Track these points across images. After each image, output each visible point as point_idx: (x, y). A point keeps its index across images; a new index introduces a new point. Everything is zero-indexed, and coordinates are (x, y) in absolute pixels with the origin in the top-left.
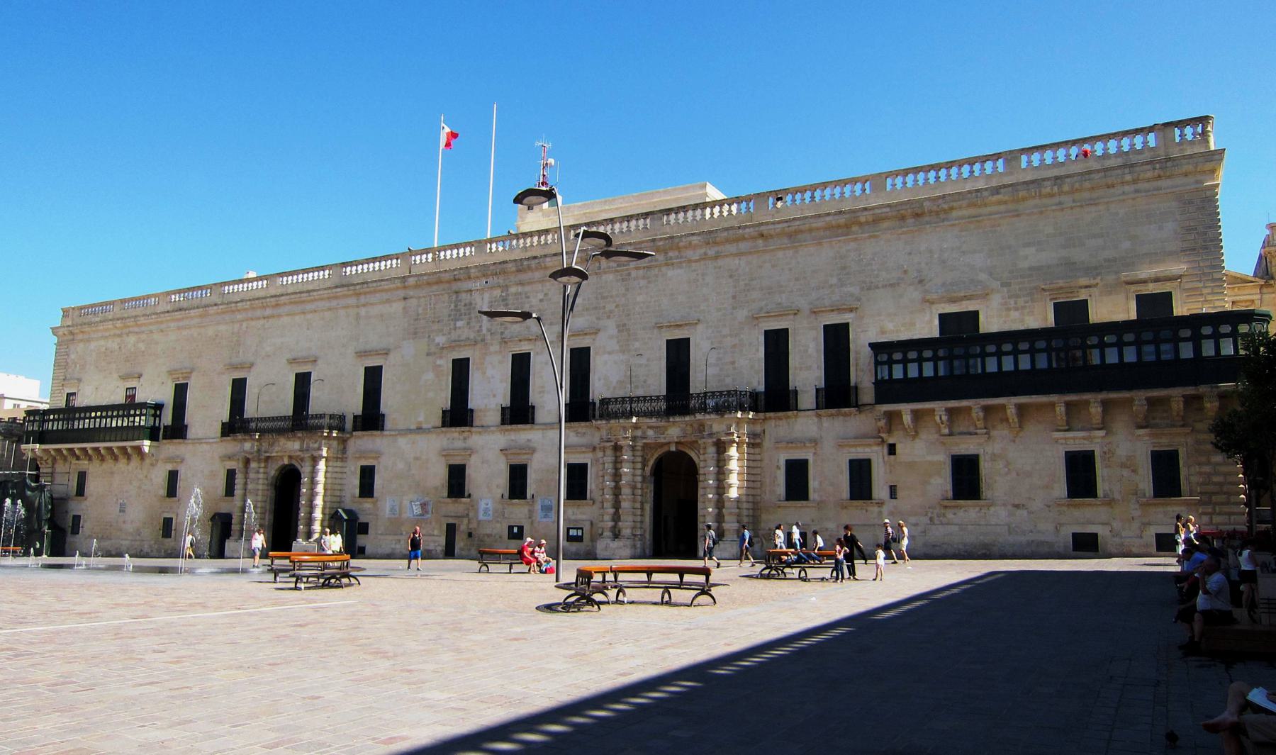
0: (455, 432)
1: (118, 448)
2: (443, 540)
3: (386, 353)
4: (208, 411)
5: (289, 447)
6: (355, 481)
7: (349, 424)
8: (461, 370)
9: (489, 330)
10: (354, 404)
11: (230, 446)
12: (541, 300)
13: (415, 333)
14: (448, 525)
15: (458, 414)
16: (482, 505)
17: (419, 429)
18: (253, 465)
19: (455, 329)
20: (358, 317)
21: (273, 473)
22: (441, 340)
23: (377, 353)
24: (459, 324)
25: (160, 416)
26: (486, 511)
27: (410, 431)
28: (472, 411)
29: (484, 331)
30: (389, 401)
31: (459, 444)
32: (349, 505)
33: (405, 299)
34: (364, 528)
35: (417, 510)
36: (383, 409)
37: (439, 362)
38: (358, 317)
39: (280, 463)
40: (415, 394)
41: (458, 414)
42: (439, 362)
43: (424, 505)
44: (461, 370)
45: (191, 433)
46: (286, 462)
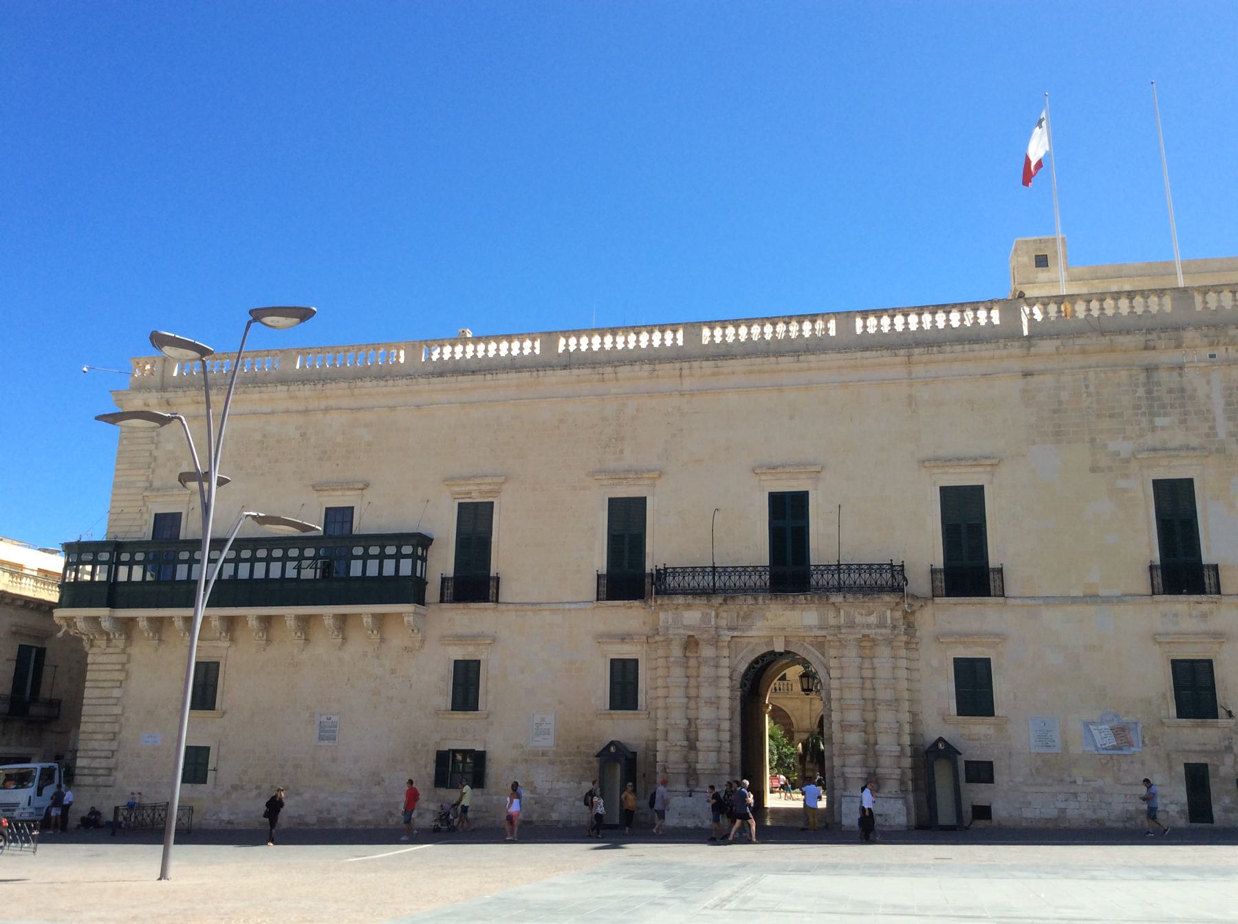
0: (1182, 606)
1: (86, 619)
3: (993, 462)
5: (783, 622)
6: (941, 690)
7: (919, 582)
11: (628, 616)
17: (1121, 599)
18: (707, 652)
19: (1153, 429)
20: (911, 401)
21: (743, 667)
23: (976, 461)
24: (1159, 421)
25: (424, 559)
27: (1074, 600)
28: (1215, 568)
29: (1222, 433)
31: (1189, 624)
32: (934, 729)
33: (1027, 374)
35: (1104, 737)
36: (993, 561)
37: (1122, 483)
38: (911, 401)
42: (1122, 483)
43: (1120, 731)
45: (507, 592)
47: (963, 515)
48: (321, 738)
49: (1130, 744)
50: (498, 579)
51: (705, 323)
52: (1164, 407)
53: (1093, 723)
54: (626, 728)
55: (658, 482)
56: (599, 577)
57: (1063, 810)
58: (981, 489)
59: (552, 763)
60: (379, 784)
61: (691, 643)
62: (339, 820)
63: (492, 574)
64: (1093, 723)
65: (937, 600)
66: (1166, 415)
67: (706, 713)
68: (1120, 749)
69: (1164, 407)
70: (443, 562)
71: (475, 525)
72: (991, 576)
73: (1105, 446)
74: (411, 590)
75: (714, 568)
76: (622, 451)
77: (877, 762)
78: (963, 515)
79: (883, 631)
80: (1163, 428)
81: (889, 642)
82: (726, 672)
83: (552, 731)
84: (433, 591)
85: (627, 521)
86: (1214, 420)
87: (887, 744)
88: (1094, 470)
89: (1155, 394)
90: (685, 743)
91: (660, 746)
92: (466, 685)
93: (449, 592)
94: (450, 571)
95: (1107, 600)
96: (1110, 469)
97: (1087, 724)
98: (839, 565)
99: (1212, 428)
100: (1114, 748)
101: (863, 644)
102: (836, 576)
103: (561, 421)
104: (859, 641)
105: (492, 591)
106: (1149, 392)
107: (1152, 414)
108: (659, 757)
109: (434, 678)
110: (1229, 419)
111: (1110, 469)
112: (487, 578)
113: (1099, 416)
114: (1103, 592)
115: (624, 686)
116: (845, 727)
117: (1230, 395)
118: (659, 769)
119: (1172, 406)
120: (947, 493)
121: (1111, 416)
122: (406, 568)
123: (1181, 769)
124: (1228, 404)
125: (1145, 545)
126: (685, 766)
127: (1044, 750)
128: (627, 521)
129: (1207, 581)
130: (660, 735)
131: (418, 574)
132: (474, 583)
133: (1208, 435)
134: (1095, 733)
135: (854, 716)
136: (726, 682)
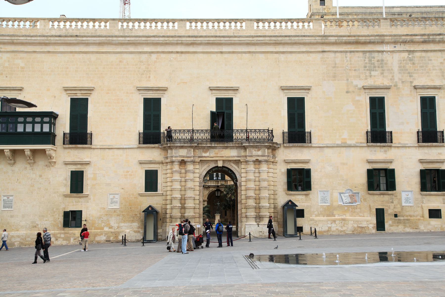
2: (374, 220)
4: (116, 123)
7: (278, 139)
8: (377, 107)
9: (400, 79)
10: (280, 125)
12: (441, 63)
13: (334, 77)
14: (377, 210)
15: (378, 134)
16: (404, 195)
18: (190, 167)
19: (371, 76)
22: (361, 83)
24: (373, 73)
25: (54, 125)
26: (407, 200)
29: (396, 79)
30: (311, 123)
34: (301, 213)
35: (346, 198)
36: (307, 129)
37: (357, 98)
39: (213, 165)
40: (338, 121)
41: (378, 134)
42: (357, 98)
43: (351, 197)
44: (377, 107)
45: (96, 141)
46: (220, 164)
47: (296, 108)
48: (4, 207)
49: (356, 201)
50: (91, 134)
51: (188, 20)
52: (375, 67)
53: (342, 193)
54: (154, 201)
55: (166, 92)
56: (139, 133)
57: (330, 227)
58: (304, 98)
59: (118, 215)
60: (35, 227)
61: (183, 163)
62: (16, 243)
63: (89, 131)
64: (342, 193)
65: (285, 145)
66: (376, 71)
67: (189, 194)
68: (352, 203)
69: (375, 67)
70: (63, 126)
71: (79, 108)
72: (306, 135)
73: (352, 82)
74: (49, 138)
75: (193, 130)
76: (149, 77)
77: (260, 211)
78: (296, 108)
79: (264, 158)
80: (375, 76)
81: (266, 161)
82: (197, 175)
83: (119, 202)
84: (59, 139)
85: (152, 108)
86: (394, 73)
87: (265, 203)
88: (347, 92)
89: (373, 62)
90: (180, 205)
91: (169, 207)
92: (77, 182)
93: (67, 139)
94: (68, 131)
95: (350, 146)
96: (353, 92)
97: (340, 194)
98: (247, 130)
99: (393, 76)
100: (350, 203)
101: (256, 163)
102: (245, 134)
103: (120, 61)
104: (254, 162)
105: (89, 139)
106: (370, 61)
107: (370, 70)
108: (168, 211)
109: (61, 178)
110: (400, 73)
111: (353, 92)
112: (86, 134)
113: (350, 70)
114: (349, 142)
115: (151, 181)
116: (247, 198)
117: (401, 63)
118: (168, 216)
119: (379, 67)
120: (290, 100)
121: (355, 70)
122: (46, 128)
123: (374, 211)
124: (400, 67)
125: (365, 124)
126: (180, 215)
127: (324, 204)
128: (152, 108)
129: (387, 137)
130: (168, 202)
131: (52, 131)
132: (79, 135)
133: (391, 79)
134: (343, 197)
135: (251, 193)
136: (198, 179)
